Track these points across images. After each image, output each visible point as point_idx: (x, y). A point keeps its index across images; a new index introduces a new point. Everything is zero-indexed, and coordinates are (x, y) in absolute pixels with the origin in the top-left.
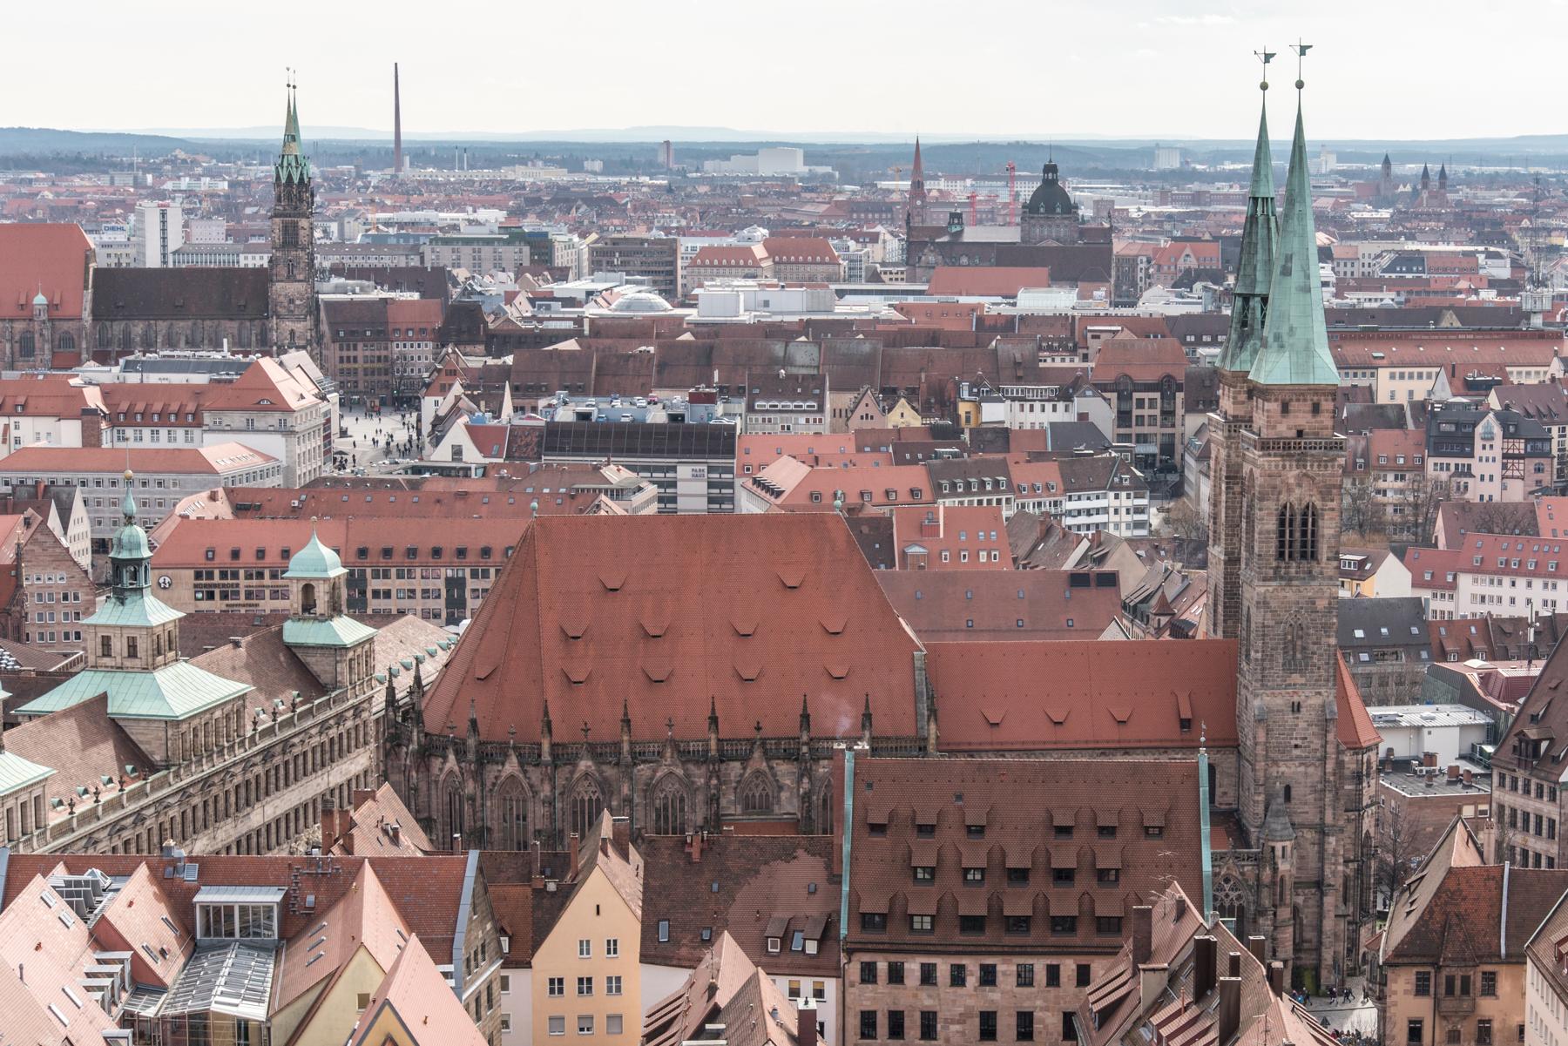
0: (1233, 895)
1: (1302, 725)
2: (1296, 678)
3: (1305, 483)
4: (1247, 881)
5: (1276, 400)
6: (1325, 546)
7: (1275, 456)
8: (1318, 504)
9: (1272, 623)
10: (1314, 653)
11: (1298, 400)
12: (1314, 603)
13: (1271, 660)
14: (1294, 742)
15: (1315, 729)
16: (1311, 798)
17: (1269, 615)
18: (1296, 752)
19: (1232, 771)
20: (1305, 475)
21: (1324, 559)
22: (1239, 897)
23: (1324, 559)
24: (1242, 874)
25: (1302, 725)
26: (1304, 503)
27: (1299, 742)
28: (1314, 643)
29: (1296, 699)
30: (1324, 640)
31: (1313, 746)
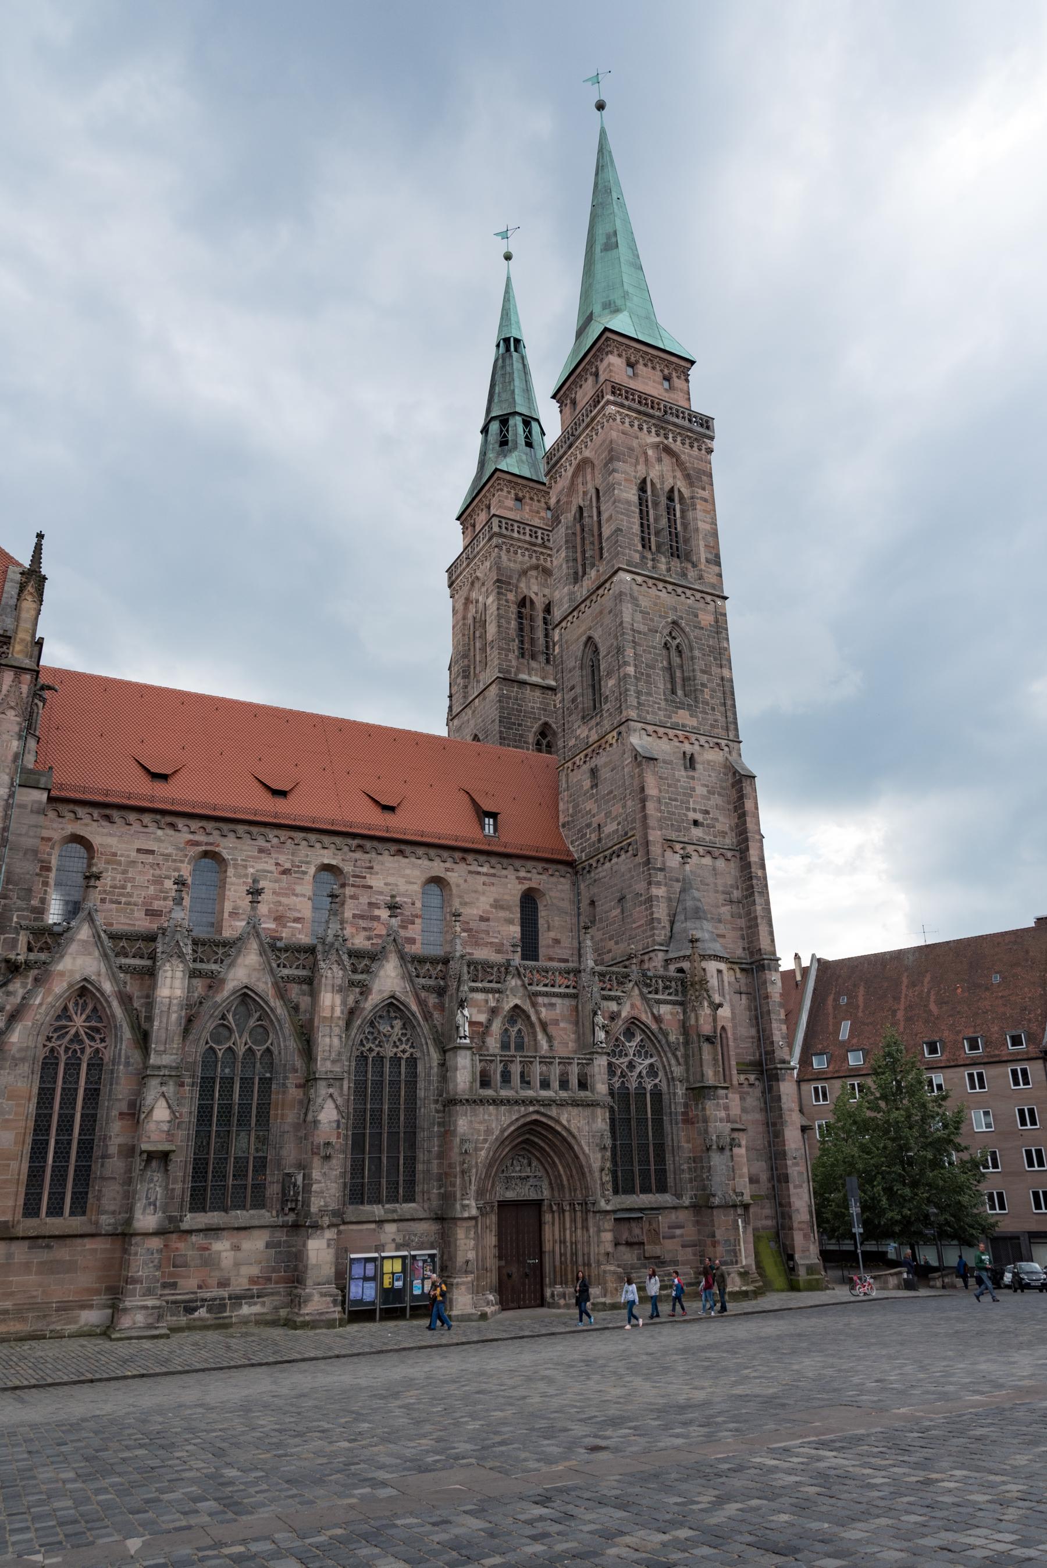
0: (643, 1064)
1: (700, 790)
2: (683, 717)
3: (667, 459)
4: (666, 1035)
5: (620, 356)
6: (702, 543)
7: (630, 408)
8: (686, 493)
9: (643, 628)
10: (703, 685)
11: (645, 365)
12: (696, 616)
13: (648, 682)
14: (692, 816)
15: (716, 800)
16: (725, 910)
17: (639, 617)
18: (697, 832)
19: (566, 905)
20: (667, 450)
21: (703, 560)
22: (652, 1071)
23: (703, 560)
24: (658, 1019)
25: (700, 790)
26: (667, 488)
27: (699, 817)
28: (704, 672)
29: (687, 747)
30: (715, 670)
31: (719, 827)
